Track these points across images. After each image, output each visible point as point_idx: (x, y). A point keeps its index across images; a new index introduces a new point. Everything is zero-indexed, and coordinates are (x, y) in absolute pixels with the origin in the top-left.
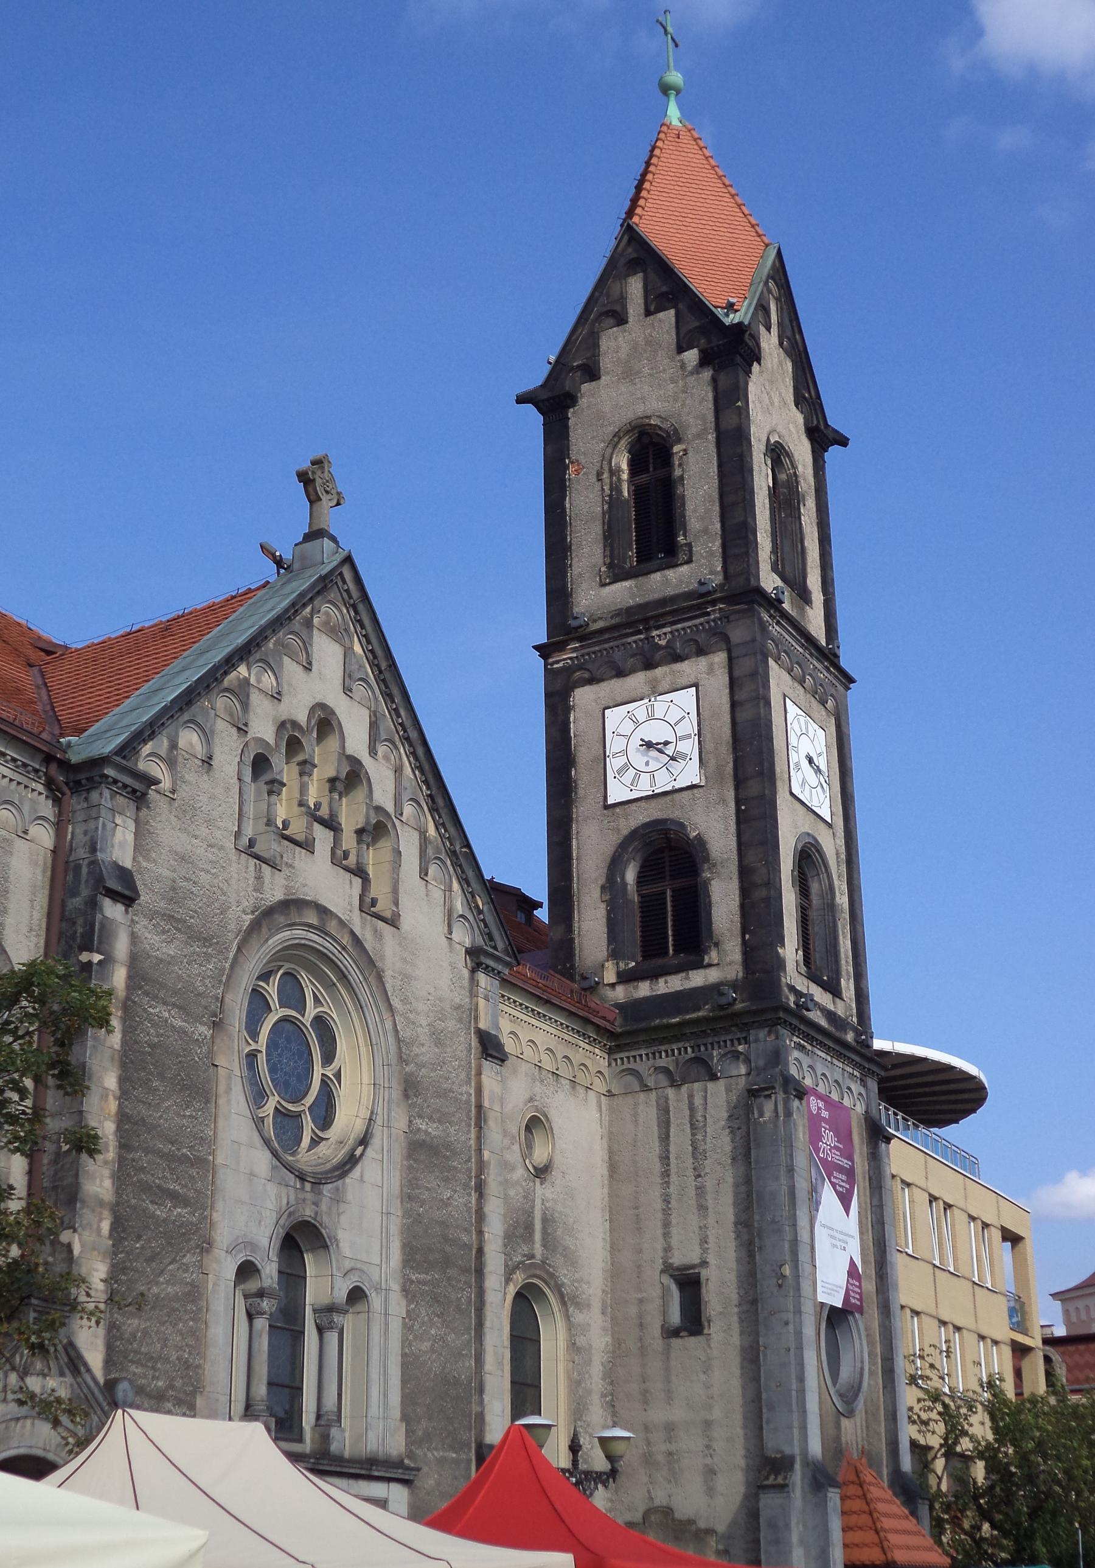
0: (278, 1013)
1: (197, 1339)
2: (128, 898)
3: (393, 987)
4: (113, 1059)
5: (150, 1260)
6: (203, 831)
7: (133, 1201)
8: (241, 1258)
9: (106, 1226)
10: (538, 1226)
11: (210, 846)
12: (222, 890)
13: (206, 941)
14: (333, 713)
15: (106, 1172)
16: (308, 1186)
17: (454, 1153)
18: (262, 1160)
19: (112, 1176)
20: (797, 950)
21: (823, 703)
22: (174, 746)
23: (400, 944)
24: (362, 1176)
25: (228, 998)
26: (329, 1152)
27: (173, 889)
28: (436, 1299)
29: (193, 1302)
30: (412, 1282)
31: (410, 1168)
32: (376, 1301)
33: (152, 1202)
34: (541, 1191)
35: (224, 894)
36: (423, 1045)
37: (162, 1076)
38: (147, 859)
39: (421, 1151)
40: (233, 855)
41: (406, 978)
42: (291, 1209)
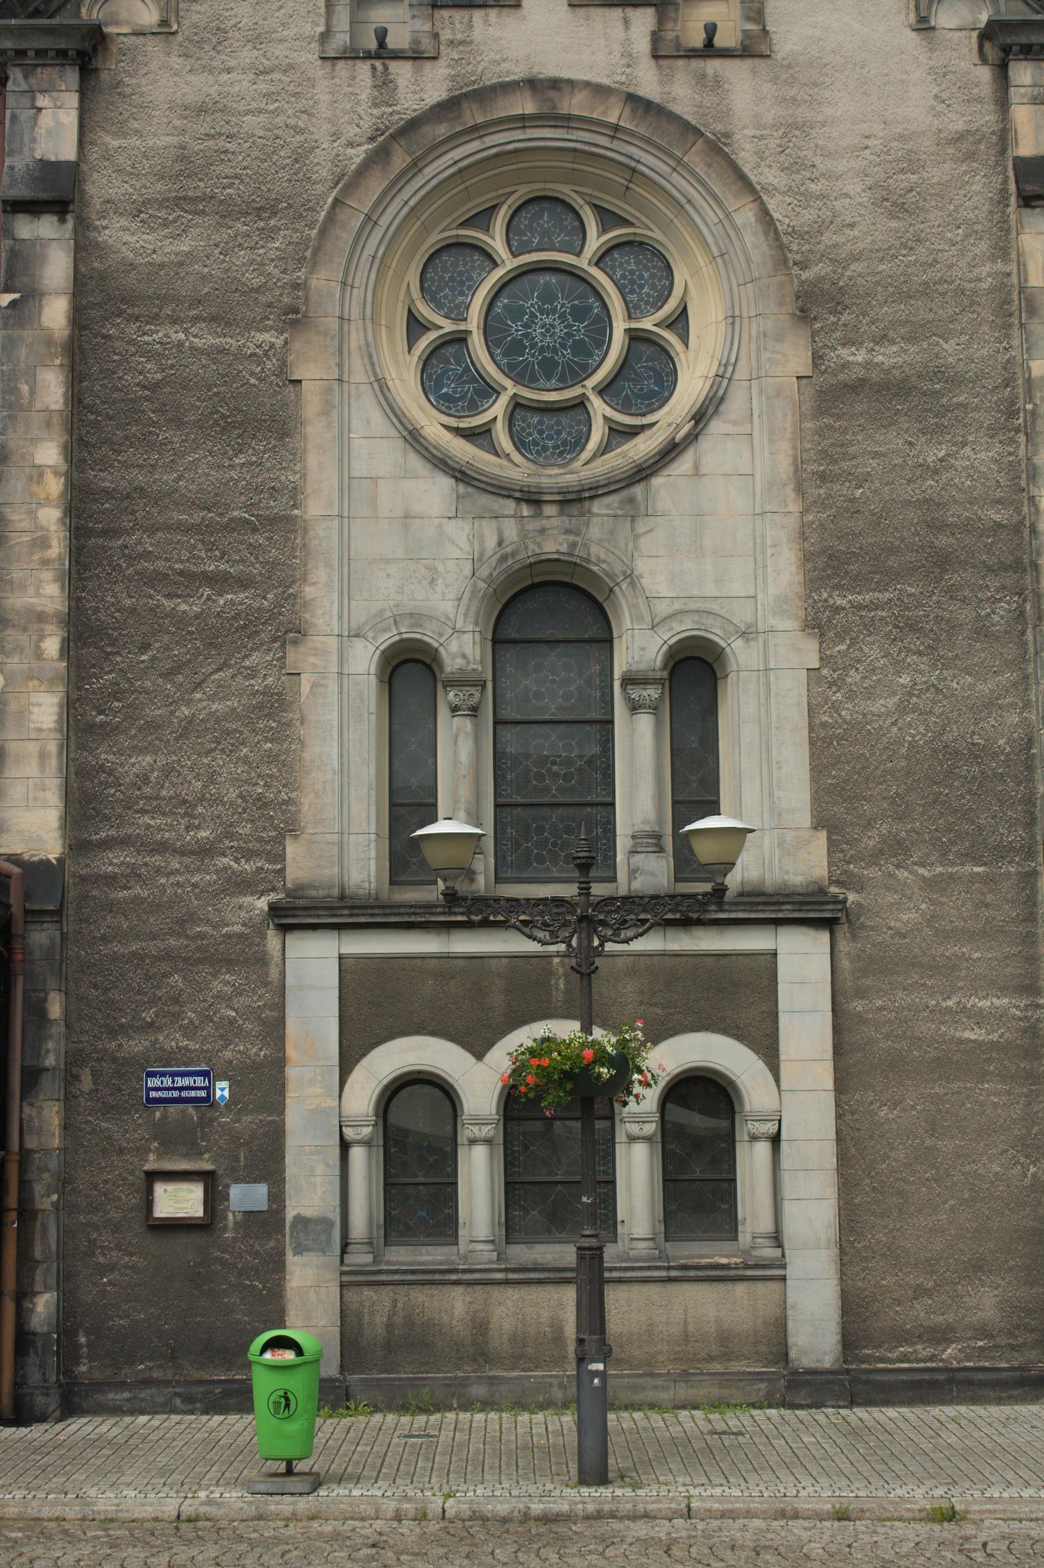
0: (509, 263)
1: (283, 764)
3: (761, 155)
4: (48, 424)
5: (168, 675)
6: (247, 55)
7: (128, 602)
8: (388, 638)
9: (52, 646)
11: (264, 72)
12: (294, 128)
15: (47, 575)
16: (550, 510)
17: (956, 381)
18: (435, 492)
19: (59, 579)
23: (775, 80)
24: (696, 467)
25: (323, 281)
26: (643, 447)
27: (183, 158)
28: (914, 627)
29: (269, 716)
30: (837, 610)
31: (820, 433)
32: (741, 656)
33: (169, 596)
35: (300, 131)
36: (852, 226)
37: (178, 422)
39: (834, 398)
40: (320, 71)
41: (794, 129)
42: (509, 550)
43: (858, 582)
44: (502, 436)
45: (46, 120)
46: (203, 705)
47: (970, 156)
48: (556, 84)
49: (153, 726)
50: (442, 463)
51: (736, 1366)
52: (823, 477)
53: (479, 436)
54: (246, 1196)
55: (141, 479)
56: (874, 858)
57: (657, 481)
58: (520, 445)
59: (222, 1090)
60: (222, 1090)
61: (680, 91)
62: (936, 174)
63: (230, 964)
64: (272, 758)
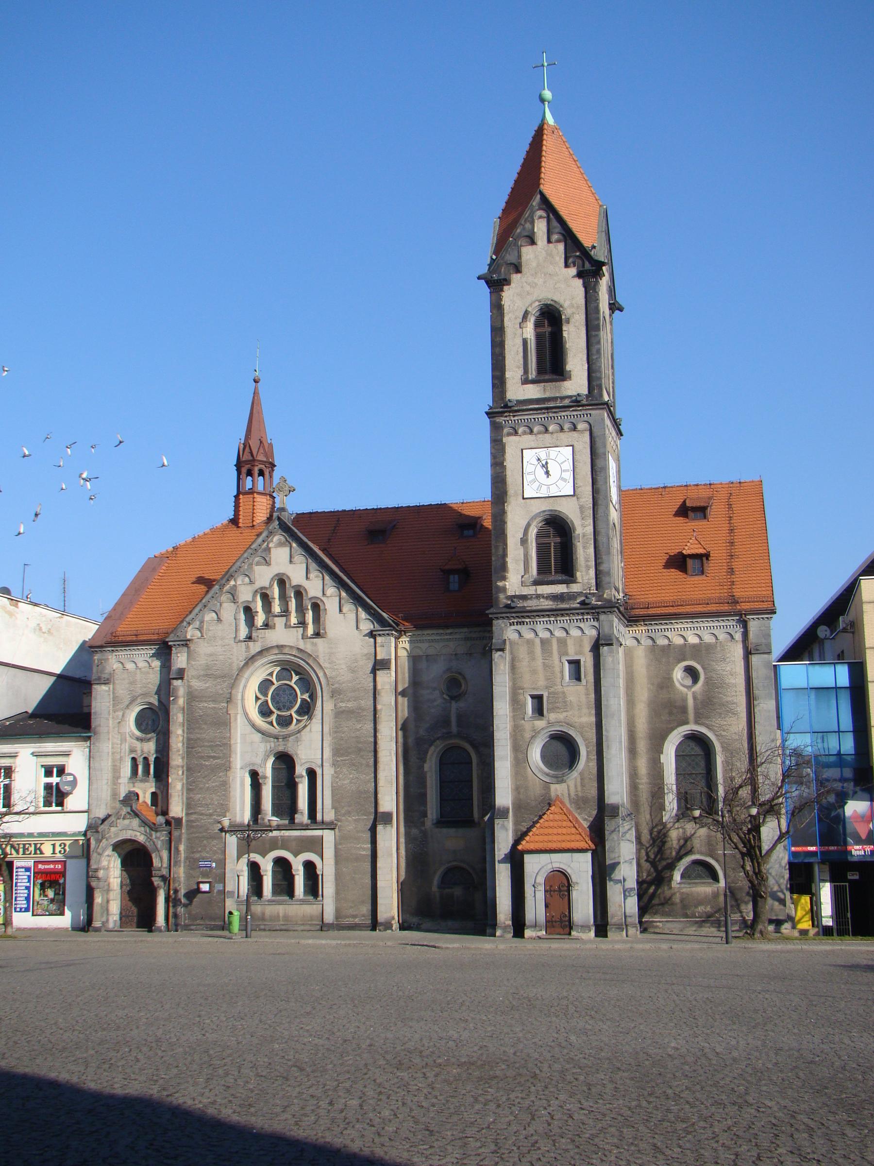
2: (182, 678)
6: (220, 642)
9: (180, 773)
10: (453, 720)
13: (222, 677)
14: (284, 574)
17: (363, 710)
20: (522, 577)
21: (574, 428)
22: (202, 622)
34: (454, 705)
37: (206, 724)
38: (195, 660)
40: (234, 645)
43: (342, 755)
44: (275, 723)
45: (180, 659)
46: (211, 784)
47: (369, 659)
48: (282, 646)
49: (201, 789)
50: (259, 731)
51: (314, 922)
52: (336, 732)
53: (271, 723)
54: (219, 887)
55: (199, 736)
56: (344, 815)
57: (302, 733)
58: (278, 724)
59: (214, 865)
60: (214, 865)
61: (307, 646)
62: (361, 663)
63: (215, 838)
64: (224, 795)
